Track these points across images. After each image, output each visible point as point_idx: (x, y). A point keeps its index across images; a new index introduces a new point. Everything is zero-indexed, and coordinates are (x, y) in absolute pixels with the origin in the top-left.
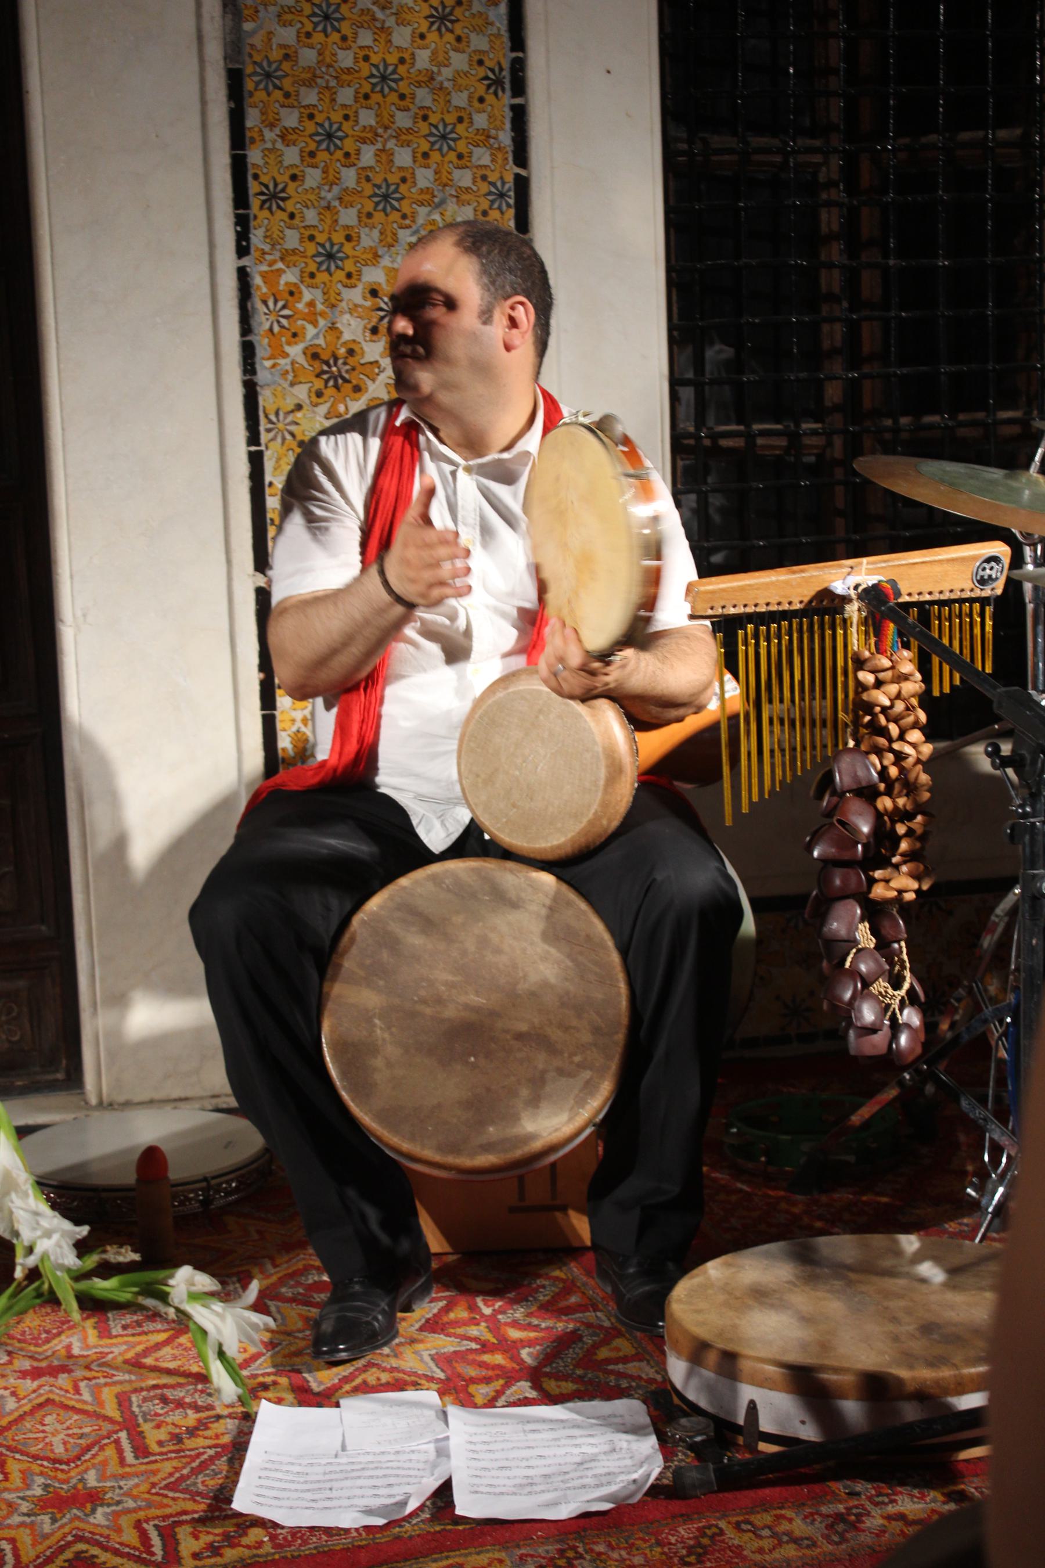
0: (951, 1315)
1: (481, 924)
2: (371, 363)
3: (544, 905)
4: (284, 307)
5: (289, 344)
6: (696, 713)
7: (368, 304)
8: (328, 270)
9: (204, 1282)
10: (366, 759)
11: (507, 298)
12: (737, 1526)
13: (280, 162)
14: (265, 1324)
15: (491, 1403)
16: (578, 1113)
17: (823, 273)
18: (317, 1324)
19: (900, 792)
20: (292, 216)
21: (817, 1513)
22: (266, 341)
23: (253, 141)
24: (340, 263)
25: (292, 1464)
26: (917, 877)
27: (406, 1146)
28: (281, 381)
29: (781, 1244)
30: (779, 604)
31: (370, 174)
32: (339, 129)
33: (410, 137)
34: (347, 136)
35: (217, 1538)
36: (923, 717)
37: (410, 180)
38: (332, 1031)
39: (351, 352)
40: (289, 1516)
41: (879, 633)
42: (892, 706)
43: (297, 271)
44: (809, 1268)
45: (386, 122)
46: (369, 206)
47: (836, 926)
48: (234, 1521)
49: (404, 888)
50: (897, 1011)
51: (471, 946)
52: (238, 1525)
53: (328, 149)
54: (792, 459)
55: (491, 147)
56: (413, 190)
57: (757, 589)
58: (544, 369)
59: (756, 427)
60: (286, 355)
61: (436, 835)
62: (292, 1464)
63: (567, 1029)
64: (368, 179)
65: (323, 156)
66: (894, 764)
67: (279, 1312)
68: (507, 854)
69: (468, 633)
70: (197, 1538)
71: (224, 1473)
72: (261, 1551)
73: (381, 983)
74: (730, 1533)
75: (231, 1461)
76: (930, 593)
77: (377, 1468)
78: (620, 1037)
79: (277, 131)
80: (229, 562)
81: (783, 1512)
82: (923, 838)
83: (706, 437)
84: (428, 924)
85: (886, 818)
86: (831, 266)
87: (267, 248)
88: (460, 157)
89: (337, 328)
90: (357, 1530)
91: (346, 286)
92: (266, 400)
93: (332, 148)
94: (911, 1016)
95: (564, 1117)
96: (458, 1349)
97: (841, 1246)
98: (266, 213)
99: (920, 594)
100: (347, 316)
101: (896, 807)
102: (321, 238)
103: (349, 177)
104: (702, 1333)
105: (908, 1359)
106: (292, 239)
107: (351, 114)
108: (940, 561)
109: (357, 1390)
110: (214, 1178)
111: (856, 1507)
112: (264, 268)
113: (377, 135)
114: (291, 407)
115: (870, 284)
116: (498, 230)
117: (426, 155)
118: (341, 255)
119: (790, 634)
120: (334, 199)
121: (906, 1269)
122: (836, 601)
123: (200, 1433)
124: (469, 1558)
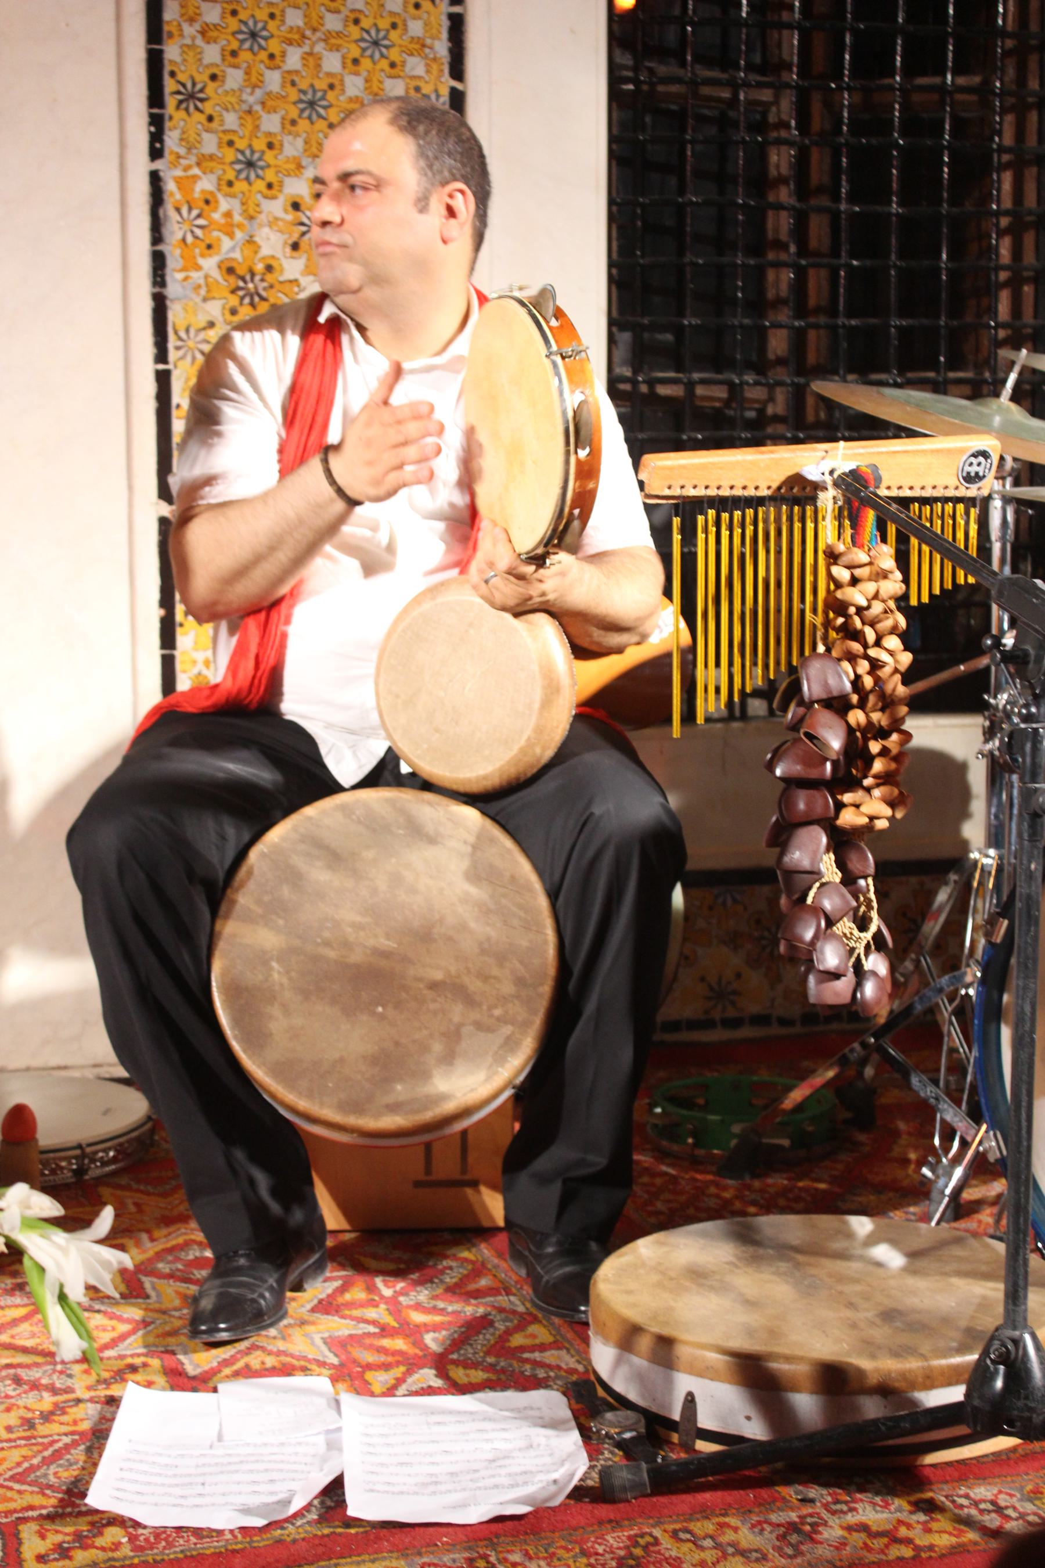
0: (913, 1302)
1: (393, 860)
2: (291, 281)
3: (465, 842)
4: (199, 216)
5: (202, 256)
6: (638, 644)
7: (289, 217)
8: (247, 179)
9: (47, 1206)
10: (272, 681)
11: (444, 183)
12: (674, 1535)
13: (200, 60)
14: (120, 1263)
15: (390, 1392)
16: (496, 1073)
17: (770, 214)
18: (196, 1300)
19: (875, 704)
20: (210, 119)
21: (766, 1522)
22: (178, 252)
23: (171, 35)
24: (260, 172)
25: (160, 1455)
26: (892, 804)
27: (303, 1104)
28: (193, 296)
29: (719, 1223)
30: (744, 488)
31: (296, 79)
32: (264, 28)
33: (339, 42)
34: (272, 36)
35: (68, 1538)
36: (902, 622)
37: (338, 87)
38: (224, 973)
39: (269, 268)
40: (153, 1514)
41: (856, 525)
42: (869, 607)
43: (213, 178)
44: (751, 1249)
45: (315, 24)
46: (294, 113)
47: (798, 856)
48: (89, 1518)
49: (310, 818)
50: (863, 956)
51: (382, 884)
52: (92, 1524)
53: (251, 49)
54: (732, 413)
55: (426, 57)
56: (342, 98)
57: (721, 468)
58: (478, 266)
59: (696, 376)
60: (198, 268)
61: (347, 763)
62: (160, 1455)
63: (486, 978)
64: (293, 84)
65: (245, 56)
66: (869, 673)
67: (154, 1288)
68: (427, 786)
69: (390, 548)
70: (43, 1537)
71: (81, 1463)
72: (117, 1554)
73: (281, 922)
74: (666, 1542)
75: (89, 1450)
76: (911, 488)
77: (257, 1461)
78: (546, 989)
79: (197, 26)
80: (130, 488)
81: (727, 1520)
82: (898, 758)
83: (644, 382)
84: (335, 858)
85: (858, 734)
86: (779, 207)
87: (182, 151)
88: (393, 65)
89: (254, 242)
90: (231, 1531)
91: (266, 197)
92: (175, 315)
93: (256, 48)
94: (877, 964)
95: (481, 1075)
96: (354, 1332)
97: (788, 1227)
98: (182, 114)
99: (900, 488)
100: (266, 230)
101: (870, 723)
102: (241, 144)
103: (273, 80)
104: (634, 1315)
105: (870, 1348)
106: (210, 144)
107: (277, 13)
108: (924, 452)
109: (237, 1374)
110: (90, 1145)
111: (811, 1515)
112: (179, 173)
113: (304, 36)
114: (203, 324)
115: (818, 228)
116: (434, 109)
117: (356, 62)
118: (261, 163)
119: (755, 523)
120: (256, 103)
121: (858, 1252)
122: (808, 489)
123: (56, 1418)
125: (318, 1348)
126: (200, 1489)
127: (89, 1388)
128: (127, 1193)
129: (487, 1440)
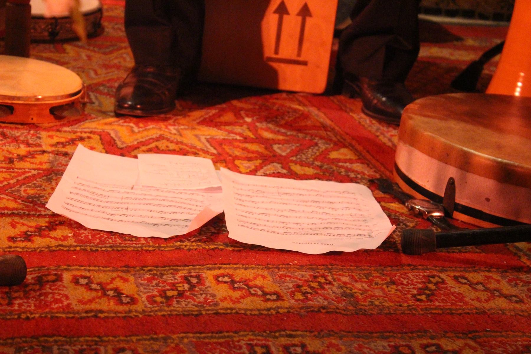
12: (456, 278)
15: (253, 172)
25: (98, 189)
62: (98, 189)
70: (13, 226)
72: (65, 243)
74: (451, 283)
77: (164, 200)
90: (145, 239)
96: (226, 138)
109: (150, 151)
123: (28, 160)
124: (238, 271)
125: (203, 143)
126: (125, 212)
127: (52, 146)
128: (81, 50)
129: (320, 207)
